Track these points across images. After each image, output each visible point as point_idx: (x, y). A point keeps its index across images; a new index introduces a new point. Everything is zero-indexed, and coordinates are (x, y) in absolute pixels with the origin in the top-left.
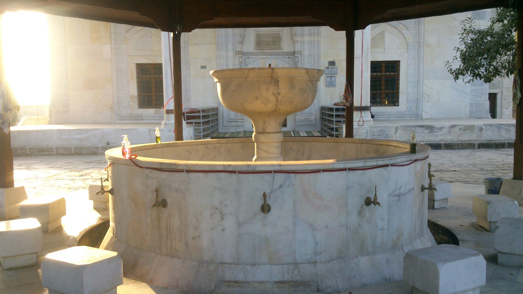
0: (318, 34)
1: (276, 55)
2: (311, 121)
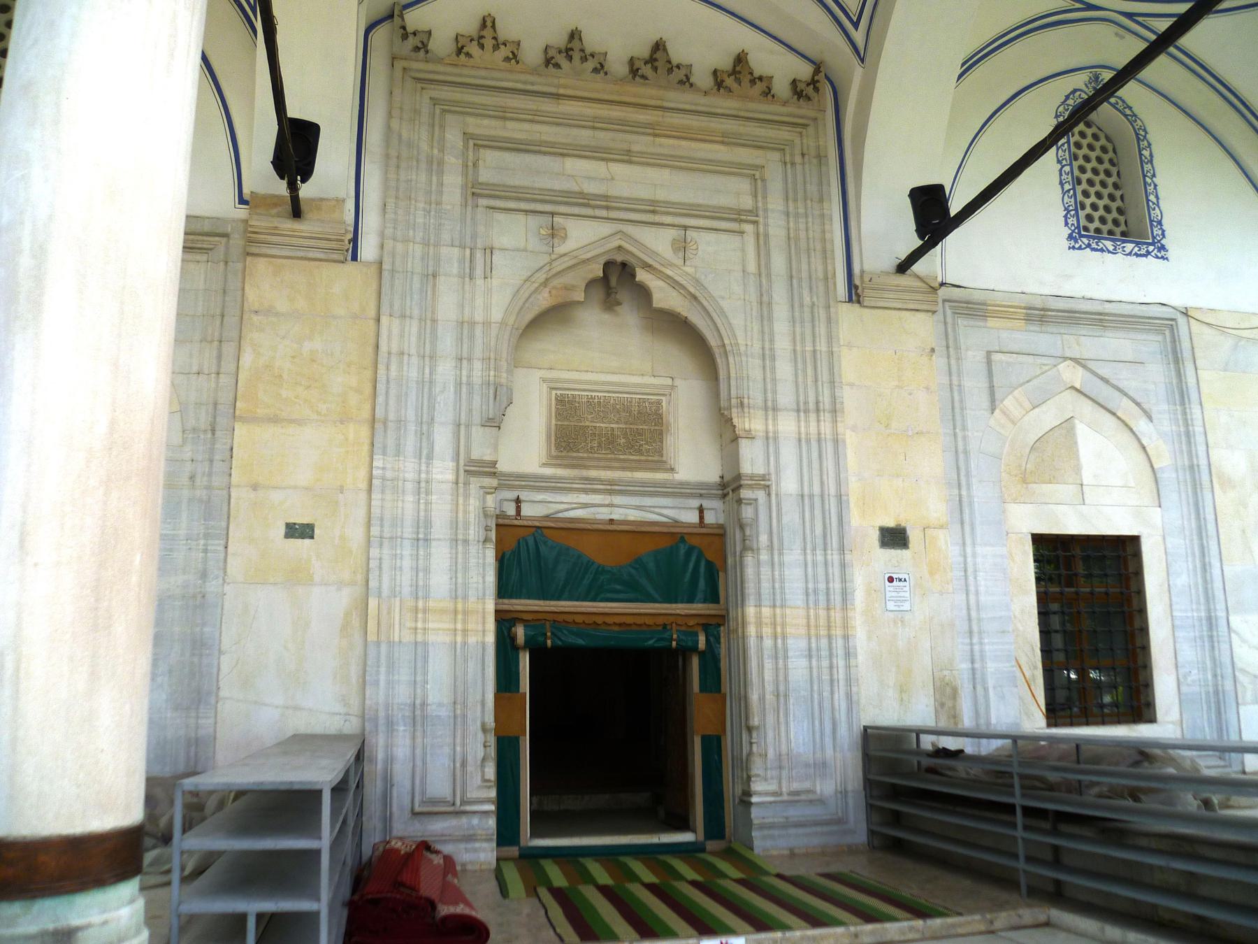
0: (834, 411)
1: (643, 494)
2: (821, 801)
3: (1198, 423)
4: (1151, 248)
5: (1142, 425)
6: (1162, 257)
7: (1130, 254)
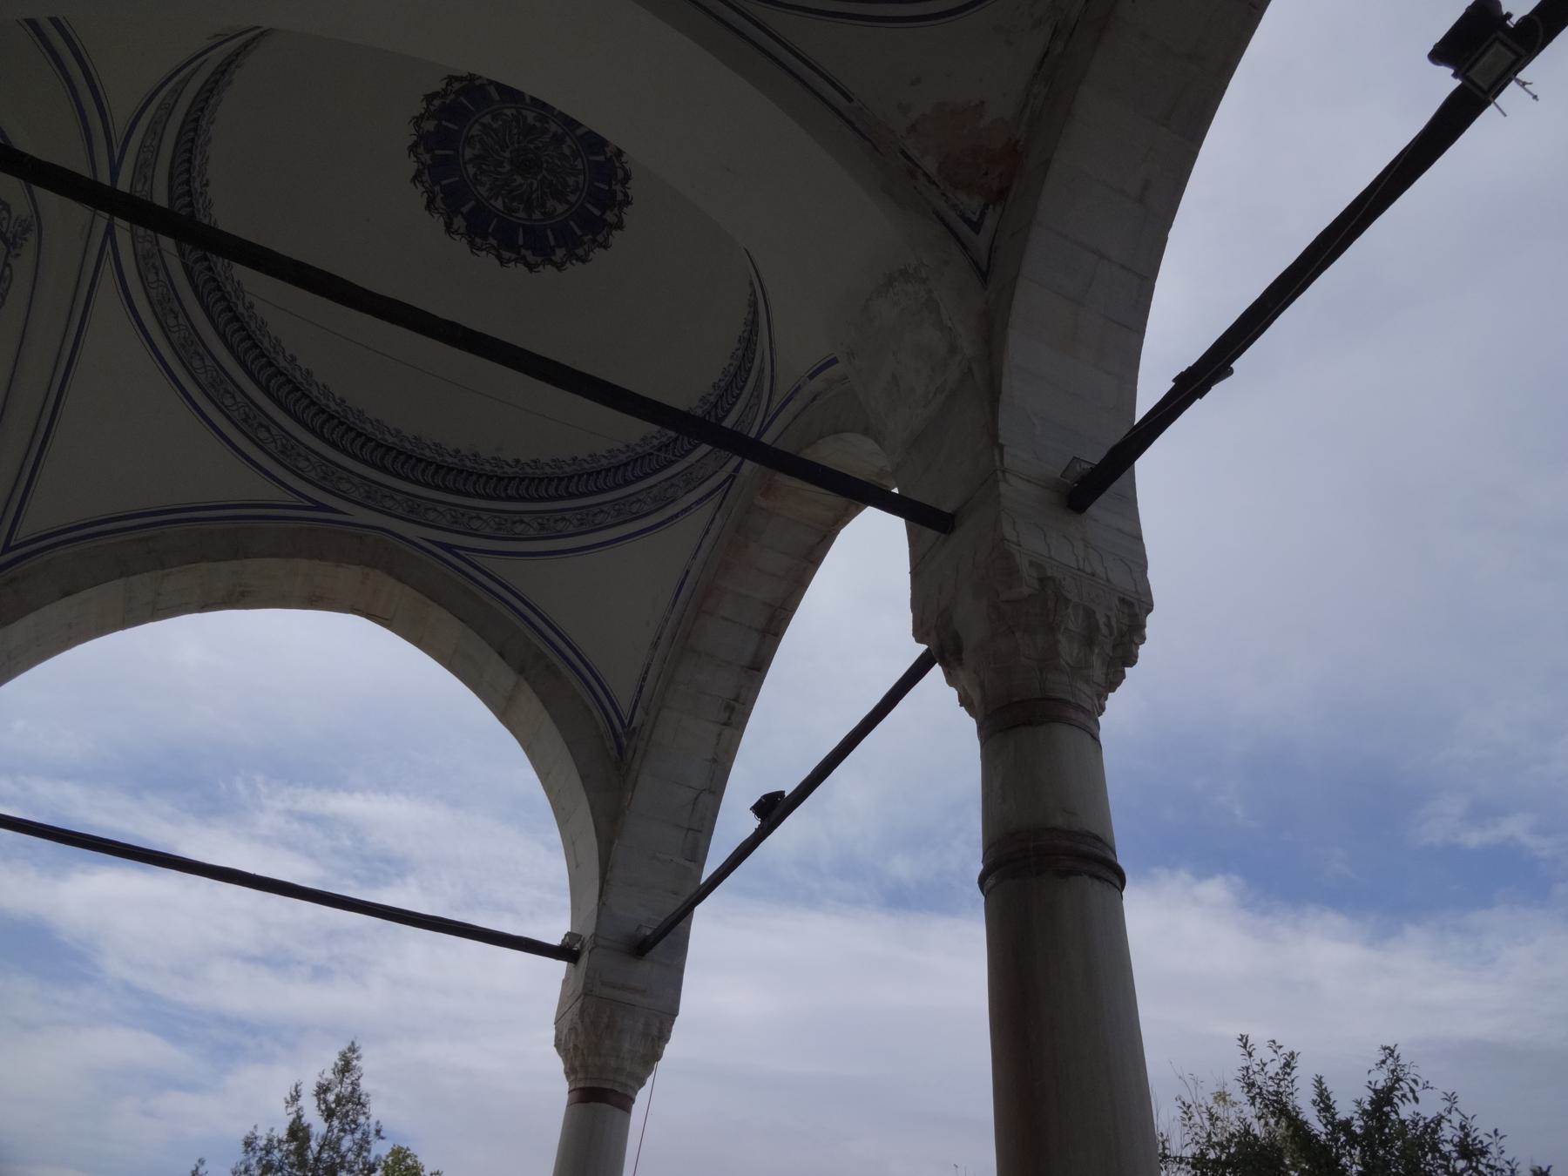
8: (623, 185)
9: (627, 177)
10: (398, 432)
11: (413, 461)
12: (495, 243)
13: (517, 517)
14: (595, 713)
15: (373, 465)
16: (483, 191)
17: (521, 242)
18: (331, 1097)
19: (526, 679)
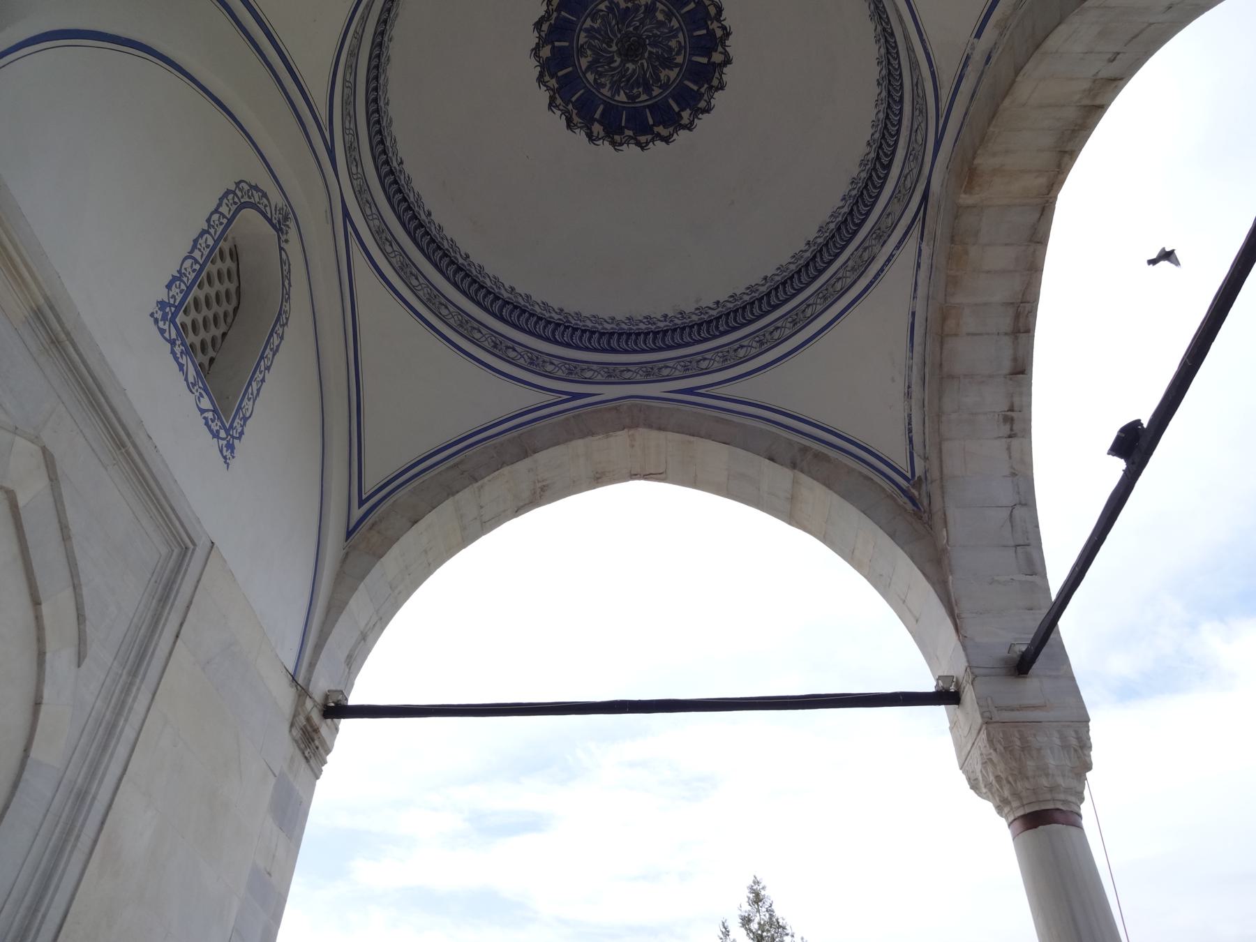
3: (135, 719)
4: (222, 434)
5: (60, 659)
6: (225, 458)
7: (202, 411)
8: (719, 21)
9: (720, 10)
10: (613, 319)
11: (633, 337)
12: (630, 133)
13: (736, 346)
14: (872, 476)
15: (604, 351)
16: (605, 91)
17: (651, 122)
18: (754, 926)
19: (802, 471)
